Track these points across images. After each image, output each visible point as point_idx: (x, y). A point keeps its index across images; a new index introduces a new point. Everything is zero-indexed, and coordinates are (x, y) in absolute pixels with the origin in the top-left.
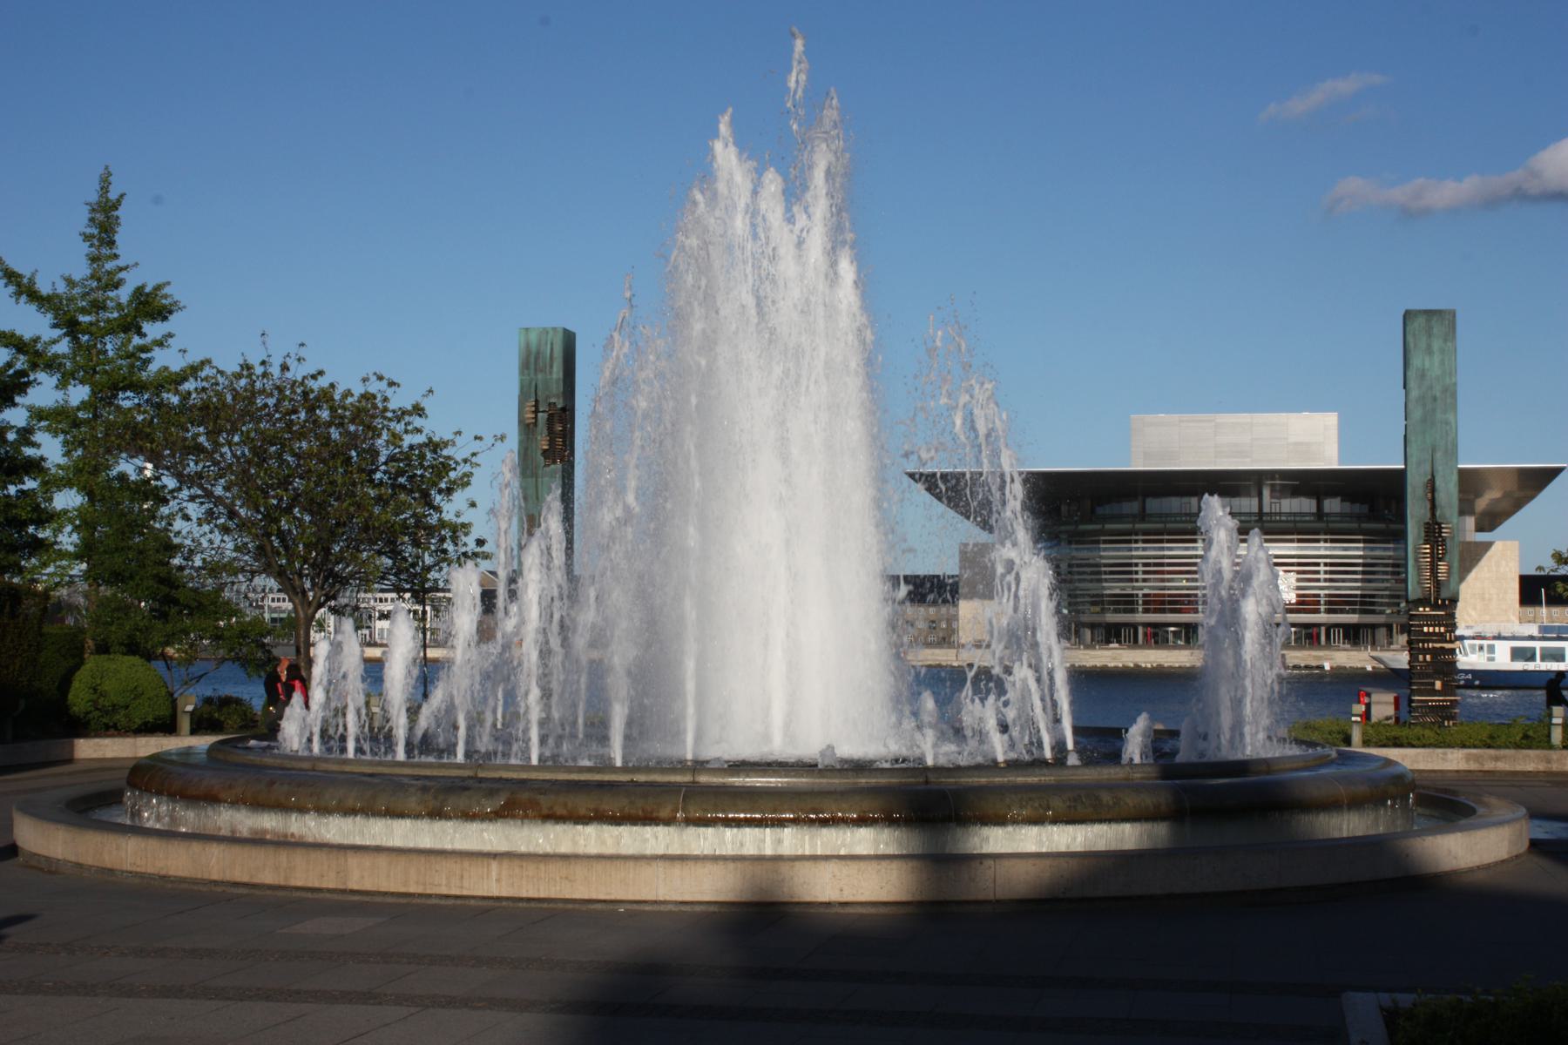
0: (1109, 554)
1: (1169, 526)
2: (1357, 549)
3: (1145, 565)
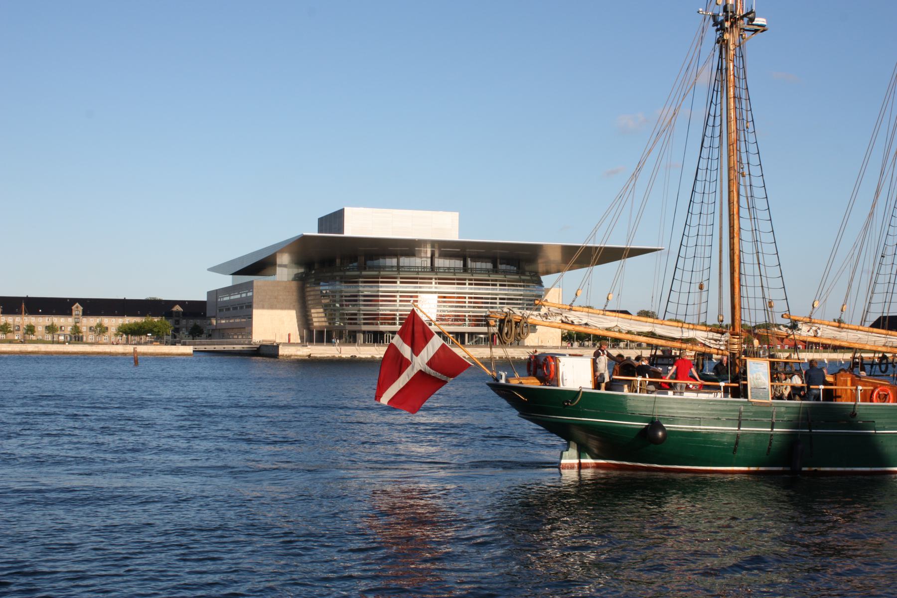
0: (365, 290)
1: (382, 273)
2: (520, 290)
3: (470, 298)
